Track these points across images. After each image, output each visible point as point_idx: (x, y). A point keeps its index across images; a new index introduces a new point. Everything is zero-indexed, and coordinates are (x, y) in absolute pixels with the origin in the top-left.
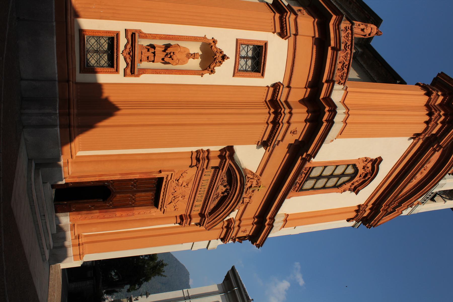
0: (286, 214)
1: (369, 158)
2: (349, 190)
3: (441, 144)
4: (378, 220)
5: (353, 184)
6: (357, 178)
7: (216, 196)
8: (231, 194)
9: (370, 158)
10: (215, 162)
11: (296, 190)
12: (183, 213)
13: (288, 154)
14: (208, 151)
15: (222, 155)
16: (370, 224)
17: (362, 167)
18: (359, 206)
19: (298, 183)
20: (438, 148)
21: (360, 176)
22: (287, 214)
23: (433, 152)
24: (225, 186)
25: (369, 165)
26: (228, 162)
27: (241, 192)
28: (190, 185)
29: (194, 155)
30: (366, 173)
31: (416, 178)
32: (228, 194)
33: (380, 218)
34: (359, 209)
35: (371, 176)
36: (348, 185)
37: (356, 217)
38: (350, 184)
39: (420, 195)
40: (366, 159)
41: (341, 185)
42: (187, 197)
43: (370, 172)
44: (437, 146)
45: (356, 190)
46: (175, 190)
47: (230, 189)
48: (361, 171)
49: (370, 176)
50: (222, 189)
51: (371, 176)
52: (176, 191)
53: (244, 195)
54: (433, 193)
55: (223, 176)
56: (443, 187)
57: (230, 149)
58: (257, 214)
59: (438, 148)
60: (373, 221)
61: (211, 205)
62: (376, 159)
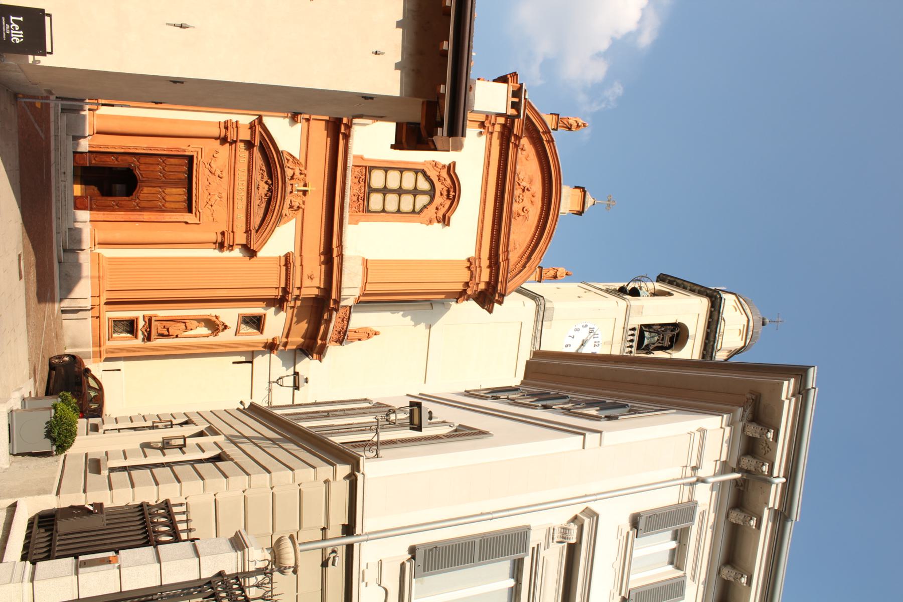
0: (364, 258)
1: (439, 162)
2: (439, 222)
3: (515, 133)
4: (505, 279)
5: (437, 209)
6: (438, 200)
7: (260, 201)
8: (275, 191)
9: (440, 163)
10: (245, 135)
11: (361, 209)
12: (224, 228)
13: (329, 139)
14: (237, 122)
15: (252, 126)
16: (499, 292)
17: (437, 178)
18: (469, 260)
19: (360, 197)
20: (517, 141)
21: (441, 194)
22: (366, 258)
23: (515, 149)
24: (266, 183)
25: (444, 174)
26: (258, 129)
27: (284, 183)
28: (225, 175)
29: (222, 126)
30: (446, 189)
31: (528, 210)
32: (272, 192)
33: (505, 277)
34: (471, 264)
35: (455, 193)
36: (431, 212)
37: (472, 278)
38: (432, 208)
39: (548, 238)
40: (434, 163)
41: (421, 211)
42: (224, 195)
43: (451, 187)
44: (514, 138)
45: (445, 220)
46: (209, 181)
47: (272, 184)
48: (439, 186)
49: (454, 194)
50: (264, 188)
51: (455, 191)
52: (210, 183)
53: (288, 182)
54: (634, 329)
55: (261, 166)
56: (642, 313)
57: (260, 118)
58: (322, 250)
59: (517, 141)
60: (499, 284)
61: (256, 220)
62: (450, 164)
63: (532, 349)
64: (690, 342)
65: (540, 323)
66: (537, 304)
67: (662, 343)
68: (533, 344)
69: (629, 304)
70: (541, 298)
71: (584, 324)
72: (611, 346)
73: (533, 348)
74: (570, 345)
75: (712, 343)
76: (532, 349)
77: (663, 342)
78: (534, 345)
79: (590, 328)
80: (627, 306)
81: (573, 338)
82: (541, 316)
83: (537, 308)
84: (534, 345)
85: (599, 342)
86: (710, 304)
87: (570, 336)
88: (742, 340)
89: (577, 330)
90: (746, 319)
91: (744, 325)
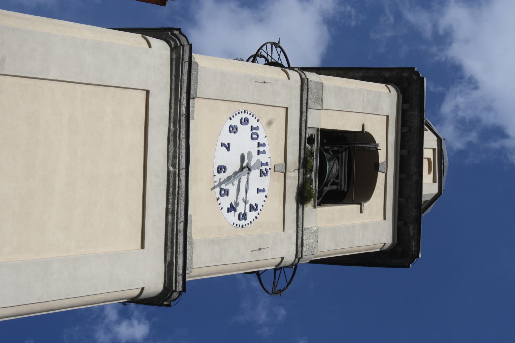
54: (311, 140)
56: (322, 99)
63: (171, 169)
64: (381, 176)
65: (184, 96)
66: (173, 45)
67: (337, 184)
68: (171, 154)
69: (304, 77)
70: (177, 32)
71: (244, 116)
72: (283, 174)
73: (174, 166)
74: (225, 168)
75: (415, 178)
76: (171, 169)
77: (339, 180)
78: (174, 157)
79: (252, 128)
80: (302, 80)
81: (228, 148)
82: (185, 77)
83: (174, 56)
84: (174, 157)
85: (267, 164)
86: (401, 96)
87: (223, 145)
88: (434, 181)
89: (233, 129)
90: (436, 138)
91: (434, 150)
